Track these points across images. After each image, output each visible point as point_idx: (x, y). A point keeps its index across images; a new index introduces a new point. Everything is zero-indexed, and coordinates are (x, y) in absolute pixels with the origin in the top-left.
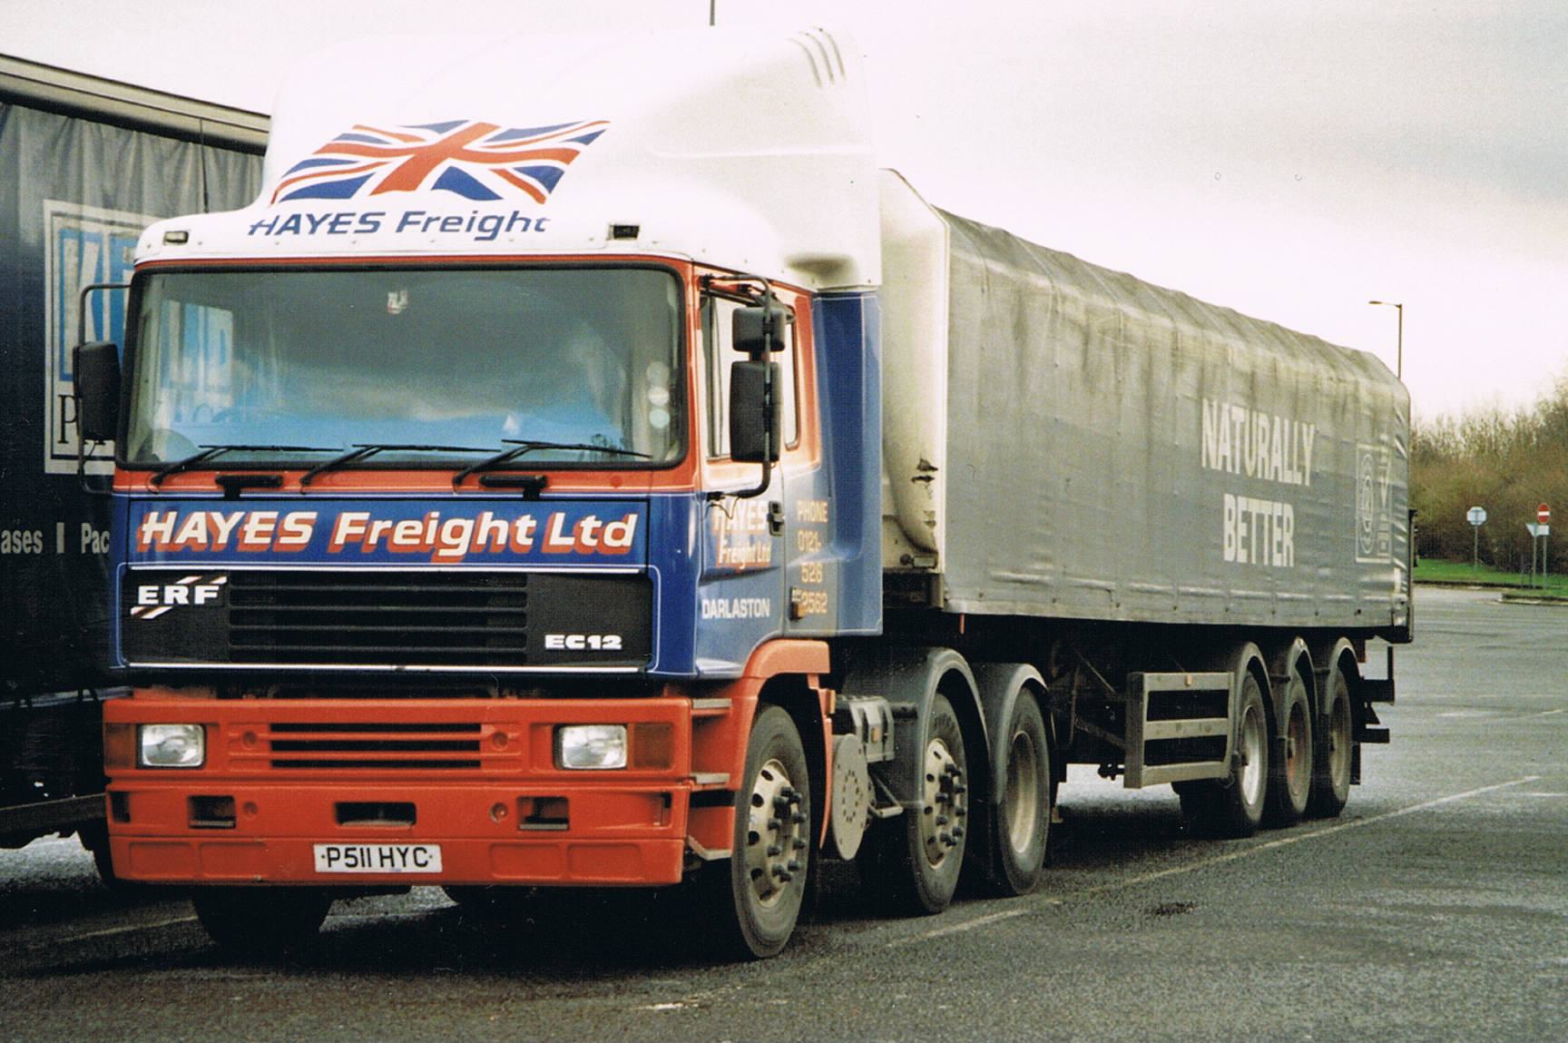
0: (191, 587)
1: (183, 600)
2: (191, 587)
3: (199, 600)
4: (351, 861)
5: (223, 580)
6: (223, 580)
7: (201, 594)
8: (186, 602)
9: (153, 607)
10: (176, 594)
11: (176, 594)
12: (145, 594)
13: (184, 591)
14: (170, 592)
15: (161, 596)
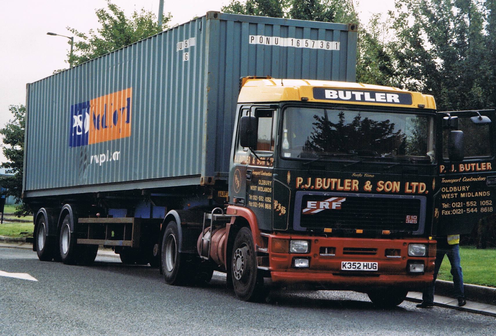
0: (331, 203)
1: (327, 207)
2: (331, 203)
3: (334, 207)
4: (354, 267)
5: (344, 200)
6: (344, 200)
7: (334, 206)
8: (328, 208)
9: (315, 209)
10: (324, 205)
11: (324, 205)
12: (310, 204)
13: (328, 204)
14: (322, 204)
15: (318, 207)
